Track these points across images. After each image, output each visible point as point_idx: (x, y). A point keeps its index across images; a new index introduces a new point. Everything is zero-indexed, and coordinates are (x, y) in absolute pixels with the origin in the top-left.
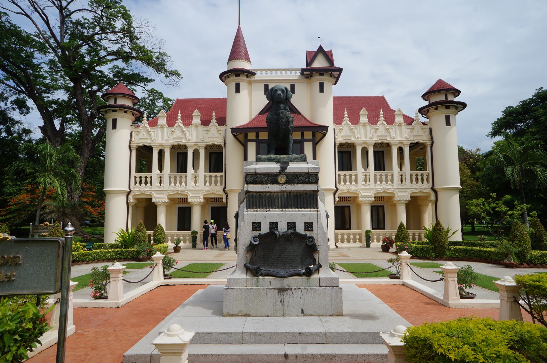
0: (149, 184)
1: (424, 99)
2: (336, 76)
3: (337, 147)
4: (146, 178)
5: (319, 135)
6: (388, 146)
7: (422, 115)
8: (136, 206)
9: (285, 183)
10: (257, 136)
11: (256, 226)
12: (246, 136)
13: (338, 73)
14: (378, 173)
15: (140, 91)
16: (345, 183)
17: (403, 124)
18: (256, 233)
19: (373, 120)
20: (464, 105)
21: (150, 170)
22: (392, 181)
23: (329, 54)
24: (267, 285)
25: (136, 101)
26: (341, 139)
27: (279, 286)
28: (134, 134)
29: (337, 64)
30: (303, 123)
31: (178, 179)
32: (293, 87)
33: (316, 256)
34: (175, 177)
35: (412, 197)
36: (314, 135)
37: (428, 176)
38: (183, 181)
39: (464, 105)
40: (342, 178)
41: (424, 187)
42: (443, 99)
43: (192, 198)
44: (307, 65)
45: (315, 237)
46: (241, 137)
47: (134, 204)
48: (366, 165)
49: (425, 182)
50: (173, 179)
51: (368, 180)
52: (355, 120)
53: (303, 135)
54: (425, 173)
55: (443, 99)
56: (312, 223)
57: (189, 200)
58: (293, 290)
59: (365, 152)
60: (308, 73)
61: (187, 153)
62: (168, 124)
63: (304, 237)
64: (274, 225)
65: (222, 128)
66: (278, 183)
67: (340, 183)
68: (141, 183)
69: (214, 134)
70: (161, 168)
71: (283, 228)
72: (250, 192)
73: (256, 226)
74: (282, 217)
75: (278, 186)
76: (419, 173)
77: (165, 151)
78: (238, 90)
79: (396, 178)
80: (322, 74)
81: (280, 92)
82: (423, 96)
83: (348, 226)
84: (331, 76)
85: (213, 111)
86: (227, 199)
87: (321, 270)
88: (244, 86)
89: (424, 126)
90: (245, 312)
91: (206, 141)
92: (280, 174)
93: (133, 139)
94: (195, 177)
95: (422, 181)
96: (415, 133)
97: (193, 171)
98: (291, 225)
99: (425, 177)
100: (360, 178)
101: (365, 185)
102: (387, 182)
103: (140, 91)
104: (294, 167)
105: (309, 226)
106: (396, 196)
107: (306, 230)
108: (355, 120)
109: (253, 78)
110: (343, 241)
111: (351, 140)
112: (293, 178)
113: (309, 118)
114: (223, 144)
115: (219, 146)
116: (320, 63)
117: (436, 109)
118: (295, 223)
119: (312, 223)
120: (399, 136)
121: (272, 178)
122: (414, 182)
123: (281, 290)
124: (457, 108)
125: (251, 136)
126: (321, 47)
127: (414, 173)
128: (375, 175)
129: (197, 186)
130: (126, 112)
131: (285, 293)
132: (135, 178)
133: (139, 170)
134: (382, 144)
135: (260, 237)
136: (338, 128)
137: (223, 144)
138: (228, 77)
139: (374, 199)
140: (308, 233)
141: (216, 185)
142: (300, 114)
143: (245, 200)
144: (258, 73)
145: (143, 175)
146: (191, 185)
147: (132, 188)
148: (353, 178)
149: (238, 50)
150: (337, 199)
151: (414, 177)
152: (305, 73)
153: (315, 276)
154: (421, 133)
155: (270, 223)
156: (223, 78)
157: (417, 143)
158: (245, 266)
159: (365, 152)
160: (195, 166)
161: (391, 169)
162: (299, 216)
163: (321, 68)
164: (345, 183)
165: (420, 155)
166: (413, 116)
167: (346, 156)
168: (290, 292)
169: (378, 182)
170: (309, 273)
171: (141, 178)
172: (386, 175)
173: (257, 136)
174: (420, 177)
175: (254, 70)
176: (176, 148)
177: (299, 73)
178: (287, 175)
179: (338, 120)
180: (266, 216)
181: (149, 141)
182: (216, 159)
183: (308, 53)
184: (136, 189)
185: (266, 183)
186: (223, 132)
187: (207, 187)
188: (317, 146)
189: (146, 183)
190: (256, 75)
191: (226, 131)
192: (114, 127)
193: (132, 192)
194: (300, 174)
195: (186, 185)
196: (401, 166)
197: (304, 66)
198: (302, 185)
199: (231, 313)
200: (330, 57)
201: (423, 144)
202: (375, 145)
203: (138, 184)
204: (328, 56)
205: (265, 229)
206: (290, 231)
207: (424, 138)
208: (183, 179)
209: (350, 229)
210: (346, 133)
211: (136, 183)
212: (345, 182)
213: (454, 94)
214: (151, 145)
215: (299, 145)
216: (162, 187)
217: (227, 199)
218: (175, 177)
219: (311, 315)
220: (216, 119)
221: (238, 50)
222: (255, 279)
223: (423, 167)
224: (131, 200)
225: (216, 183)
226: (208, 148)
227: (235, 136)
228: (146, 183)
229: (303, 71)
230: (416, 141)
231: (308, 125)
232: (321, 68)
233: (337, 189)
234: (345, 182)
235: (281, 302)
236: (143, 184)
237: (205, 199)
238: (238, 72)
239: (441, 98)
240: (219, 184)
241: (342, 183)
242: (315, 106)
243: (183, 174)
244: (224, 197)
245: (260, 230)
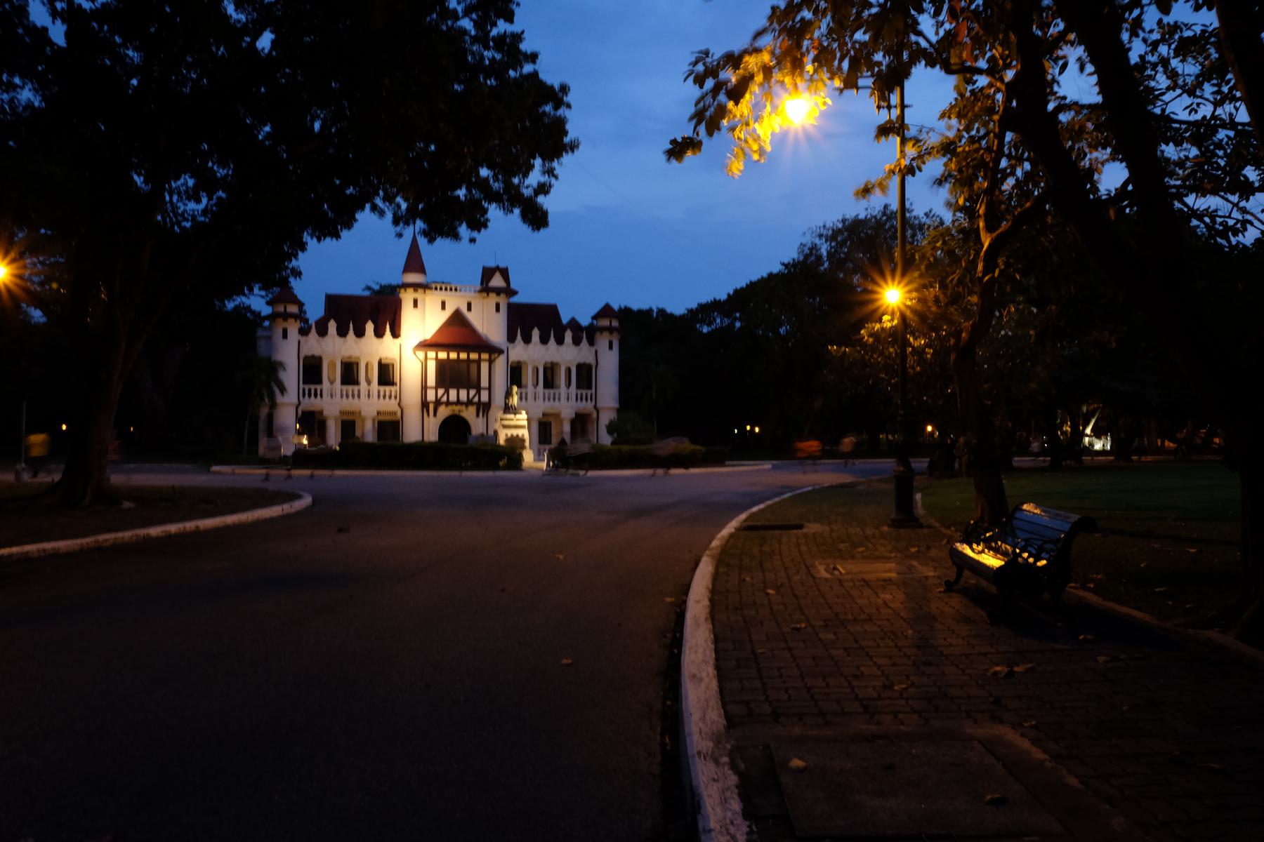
14: (547, 391)
19: (544, 340)
29: (513, 286)
52: (527, 340)
54: (589, 392)
68: (310, 395)
76: (584, 392)
79: (563, 396)
108: (527, 340)
127: (579, 392)
133: (307, 380)
179: (511, 338)
189: (316, 396)
192: (285, 336)
196: (569, 384)
204: (505, 273)
207: (590, 359)
223: (589, 387)
228: (316, 396)
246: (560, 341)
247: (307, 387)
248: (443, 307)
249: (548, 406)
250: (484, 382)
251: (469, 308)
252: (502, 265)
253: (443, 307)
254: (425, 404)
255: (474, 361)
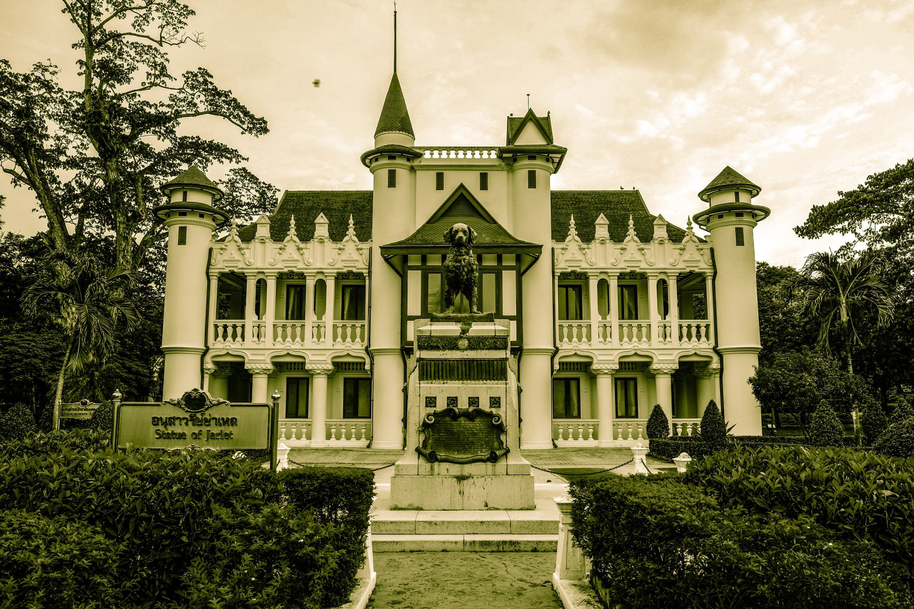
0: (239, 339)
1: (702, 199)
2: (557, 160)
3: (556, 278)
4: (235, 327)
5: (528, 260)
6: (643, 277)
7: (700, 225)
8: (214, 375)
9: (466, 349)
10: (424, 259)
11: (431, 401)
12: (405, 259)
13: (560, 156)
14: (626, 322)
15: (218, 172)
16: (570, 341)
17: (666, 242)
18: (431, 410)
19: (617, 235)
20: (766, 212)
21: (242, 316)
22: (649, 337)
23: (542, 122)
24: (444, 472)
25: (218, 197)
26: (563, 266)
27: (459, 474)
28: (214, 252)
29: (559, 141)
30: (501, 240)
31: (289, 330)
32: (484, 179)
33: (503, 438)
34: (284, 326)
35: (680, 363)
36: (518, 259)
37: (707, 326)
38: (298, 334)
39: (766, 212)
40: (565, 330)
41: (704, 346)
42: (733, 201)
43: (312, 362)
44: (509, 141)
45: (503, 416)
46: (396, 261)
47: (212, 371)
48: (604, 310)
49: (703, 338)
50: (280, 330)
51: (608, 334)
52: (587, 236)
53: (499, 259)
54: (703, 323)
55: (733, 201)
56: (499, 398)
57: (308, 367)
58: (475, 479)
59: (603, 285)
60: (510, 156)
61: (305, 286)
62: (272, 237)
63: (490, 415)
64: (453, 401)
65: (365, 246)
66: (458, 349)
67: (561, 340)
68: (225, 336)
69: (349, 255)
70: (257, 312)
71: (463, 404)
72: (422, 359)
73: (431, 401)
74: (463, 391)
75: (458, 352)
76: (694, 323)
77: (269, 282)
78: (392, 183)
79: (656, 331)
80: (532, 158)
81: (461, 234)
82: (701, 195)
83: (575, 413)
84: (548, 160)
85: (349, 213)
86: (372, 364)
87: (509, 455)
88: (402, 175)
89: (701, 246)
90: (416, 506)
91: (336, 266)
92: (461, 337)
93: (213, 261)
94: (318, 327)
95: (699, 337)
96: (686, 257)
97: (315, 318)
98: (474, 401)
99: (703, 330)
100: (595, 331)
101: (604, 342)
102: (640, 338)
103: (218, 172)
104: (478, 329)
105: (495, 402)
106: (655, 361)
107: (491, 407)
108: (587, 236)
109: (416, 163)
110: (566, 438)
111: (582, 266)
112: (477, 343)
113: (511, 234)
114: (365, 271)
115: (359, 276)
116: (530, 138)
117: (721, 217)
118: (478, 398)
119: (499, 398)
120: (659, 260)
121: (450, 343)
122: (685, 339)
123: (461, 478)
124: (754, 216)
125: (414, 260)
126: (531, 112)
128: (621, 326)
129: (321, 342)
130: (202, 216)
131: (465, 482)
132: (216, 326)
134: (633, 275)
135: (435, 414)
136: (558, 246)
137: (365, 271)
138: (377, 160)
139: (617, 367)
140: (494, 411)
141: (353, 341)
142: (495, 222)
143: (417, 369)
144: (427, 155)
145: (230, 322)
146: (309, 342)
147: (210, 344)
148: (584, 330)
149: (395, 115)
150: (557, 367)
151: (685, 330)
152: (505, 155)
153: (502, 464)
154: (697, 256)
155: (448, 398)
156: (367, 161)
157: (691, 273)
158: (417, 450)
159: (603, 285)
160: (320, 310)
161: (647, 316)
162: (483, 390)
163: (530, 146)
164: (570, 341)
165: (693, 295)
166: (684, 226)
167: (572, 293)
168: (471, 480)
169: (626, 339)
170: (494, 459)
171: (225, 327)
172: (640, 327)
173: (424, 259)
174: (694, 330)
175: (420, 148)
176: (284, 277)
177: (494, 155)
178: (469, 339)
179: (559, 233)
180: (443, 390)
181: (241, 265)
182: (354, 296)
183: (511, 120)
184: (216, 347)
185: (444, 348)
186: (366, 252)
187: (339, 345)
188: (524, 278)
189: (234, 336)
190: (425, 157)
191: (371, 249)
192: (182, 241)
193: (210, 351)
194: (486, 338)
195: (303, 340)
196: (665, 310)
197: (503, 144)
198: (487, 351)
199: (400, 506)
200: (546, 128)
201: (700, 274)
202: (621, 276)
203: (220, 338)
204: (544, 126)
205: (441, 405)
206: (471, 409)
207: (703, 266)
208: (298, 330)
209: (579, 416)
210: (573, 255)
211: (216, 336)
212: (570, 339)
213: (751, 192)
214: (245, 271)
215: (493, 276)
216: (261, 342)
217: (372, 364)
218: (284, 326)
219: (497, 509)
220: (355, 230)
221: (395, 115)
222: (428, 465)
224: (209, 365)
225: (353, 339)
226: (341, 277)
227: (387, 260)
228: (234, 336)
229: (501, 152)
230: (688, 270)
231: (508, 241)
232: (530, 146)
233: (557, 350)
234: (570, 339)
235: (460, 493)
236: (229, 338)
237: (334, 364)
238: (392, 152)
239: (728, 198)
240: (358, 339)
241: (566, 339)
242: (518, 211)
243: (298, 323)
244: (368, 361)
245: (435, 406)
246: (645, 236)
247: (221, 323)
248: (440, 186)
249: (633, 347)
250: (509, 308)
251: (484, 186)
252: (540, 114)
253: (440, 186)
254: (406, 351)
255: (489, 270)
